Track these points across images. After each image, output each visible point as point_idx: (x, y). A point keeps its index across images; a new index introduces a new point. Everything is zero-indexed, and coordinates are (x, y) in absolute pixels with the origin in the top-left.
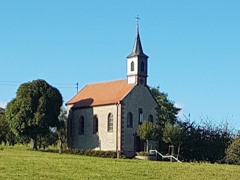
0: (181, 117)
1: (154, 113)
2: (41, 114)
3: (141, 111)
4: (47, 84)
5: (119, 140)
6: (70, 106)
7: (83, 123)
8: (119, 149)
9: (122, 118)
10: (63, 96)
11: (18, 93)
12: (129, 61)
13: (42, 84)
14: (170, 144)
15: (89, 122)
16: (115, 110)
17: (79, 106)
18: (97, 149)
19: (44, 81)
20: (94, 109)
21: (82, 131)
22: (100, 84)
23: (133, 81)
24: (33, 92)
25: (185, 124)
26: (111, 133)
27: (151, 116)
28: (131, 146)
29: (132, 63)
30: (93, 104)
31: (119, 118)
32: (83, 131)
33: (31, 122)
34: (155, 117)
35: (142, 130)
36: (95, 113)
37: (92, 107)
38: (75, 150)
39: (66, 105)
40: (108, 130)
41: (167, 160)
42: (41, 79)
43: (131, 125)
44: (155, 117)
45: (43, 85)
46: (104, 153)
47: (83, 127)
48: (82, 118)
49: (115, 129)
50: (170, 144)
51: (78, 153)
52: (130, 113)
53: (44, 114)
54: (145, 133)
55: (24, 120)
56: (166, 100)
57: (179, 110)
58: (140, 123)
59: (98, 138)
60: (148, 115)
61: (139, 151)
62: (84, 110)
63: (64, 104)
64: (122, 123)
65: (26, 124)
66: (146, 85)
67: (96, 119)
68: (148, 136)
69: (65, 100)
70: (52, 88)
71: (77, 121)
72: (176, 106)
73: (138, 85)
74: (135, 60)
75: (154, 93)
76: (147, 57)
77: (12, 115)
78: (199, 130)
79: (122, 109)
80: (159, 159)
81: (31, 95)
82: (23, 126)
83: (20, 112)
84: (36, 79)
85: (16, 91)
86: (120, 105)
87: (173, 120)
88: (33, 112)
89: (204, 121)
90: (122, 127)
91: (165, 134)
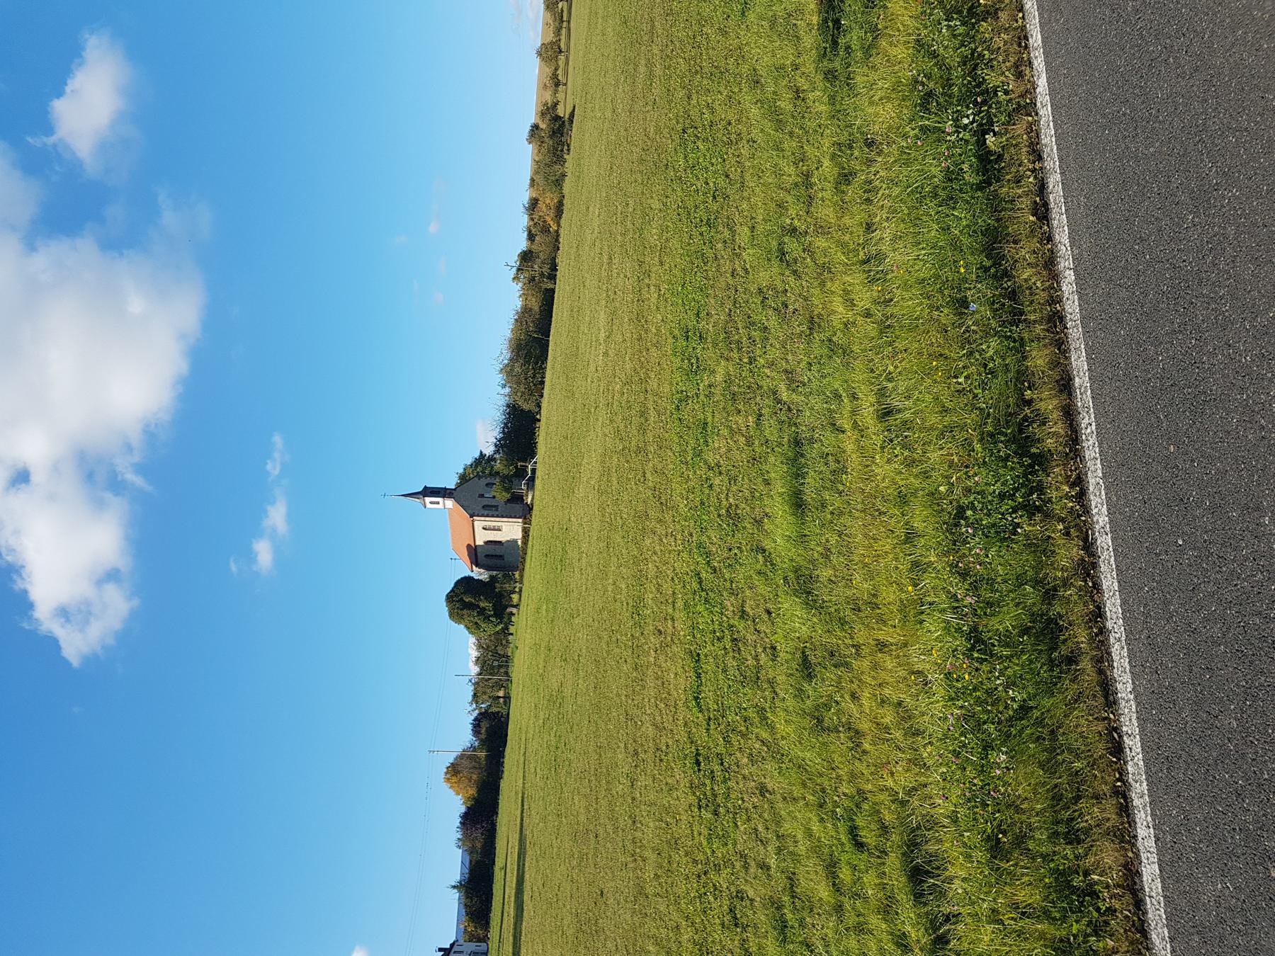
0: (489, 451)
1: (484, 481)
2: (481, 600)
3: (482, 496)
4: (450, 593)
5: (510, 520)
6: (474, 567)
7: (492, 556)
8: (520, 520)
9: (488, 516)
10: (463, 576)
11: (460, 623)
12: (429, 506)
13: (451, 598)
14: (516, 467)
15: (491, 550)
16: (479, 523)
17: (474, 557)
18: (520, 543)
19: (447, 595)
20: (477, 544)
21: (501, 557)
22: (452, 536)
23: (450, 503)
24: (458, 608)
25: (496, 446)
26: (504, 528)
27: (487, 485)
28: (518, 507)
29: (431, 503)
30: (473, 545)
31: (487, 519)
32: (501, 556)
33: (490, 611)
34: (489, 480)
35: (502, 496)
36: (482, 543)
37: (476, 546)
38: (521, 567)
39: (472, 571)
40: (500, 530)
41: (534, 471)
42: (444, 597)
43: (496, 507)
44: (489, 480)
45: (452, 597)
46: (524, 537)
47: (496, 556)
48: (487, 556)
49: (499, 524)
50: (516, 467)
51: (523, 563)
52: (483, 507)
53: (482, 598)
54: (504, 494)
55: (487, 618)
56: (471, 465)
57: (481, 452)
58: (494, 497)
59: (508, 541)
60: (486, 488)
61: (524, 500)
62: (478, 554)
63: (472, 575)
64: (493, 516)
65: (491, 616)
66: (455, 489)
67: (488, 543)
68: (507, 490)
69: (468, 573)
70: (455, 587)
71: (490, 562)
72: (477, 455)
73: (454, 498)
74: (428, 500)
75: (464, 478)
76: (425, 487)
77: (482, 630)
78: (503, 432)
79: (478, 516)
80: (532, 479)
81: (461, 610)
82: (493, 619)
83: (479, 622)
84: (445, 604)
85: (457, 625)
86: (474, 518)
87: (491, 459)
88: (479, 607)
89: (493, 427)
90: (497, 516)
91: (506, 472)
